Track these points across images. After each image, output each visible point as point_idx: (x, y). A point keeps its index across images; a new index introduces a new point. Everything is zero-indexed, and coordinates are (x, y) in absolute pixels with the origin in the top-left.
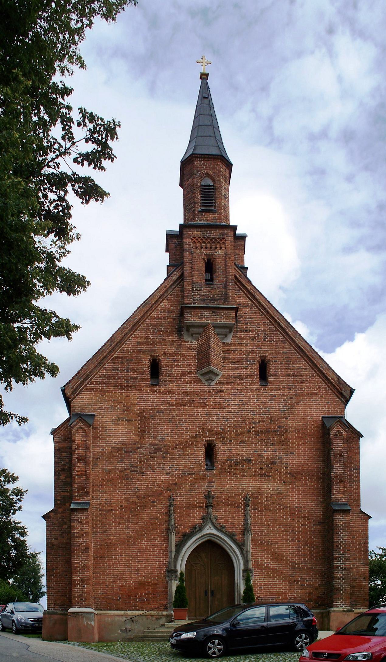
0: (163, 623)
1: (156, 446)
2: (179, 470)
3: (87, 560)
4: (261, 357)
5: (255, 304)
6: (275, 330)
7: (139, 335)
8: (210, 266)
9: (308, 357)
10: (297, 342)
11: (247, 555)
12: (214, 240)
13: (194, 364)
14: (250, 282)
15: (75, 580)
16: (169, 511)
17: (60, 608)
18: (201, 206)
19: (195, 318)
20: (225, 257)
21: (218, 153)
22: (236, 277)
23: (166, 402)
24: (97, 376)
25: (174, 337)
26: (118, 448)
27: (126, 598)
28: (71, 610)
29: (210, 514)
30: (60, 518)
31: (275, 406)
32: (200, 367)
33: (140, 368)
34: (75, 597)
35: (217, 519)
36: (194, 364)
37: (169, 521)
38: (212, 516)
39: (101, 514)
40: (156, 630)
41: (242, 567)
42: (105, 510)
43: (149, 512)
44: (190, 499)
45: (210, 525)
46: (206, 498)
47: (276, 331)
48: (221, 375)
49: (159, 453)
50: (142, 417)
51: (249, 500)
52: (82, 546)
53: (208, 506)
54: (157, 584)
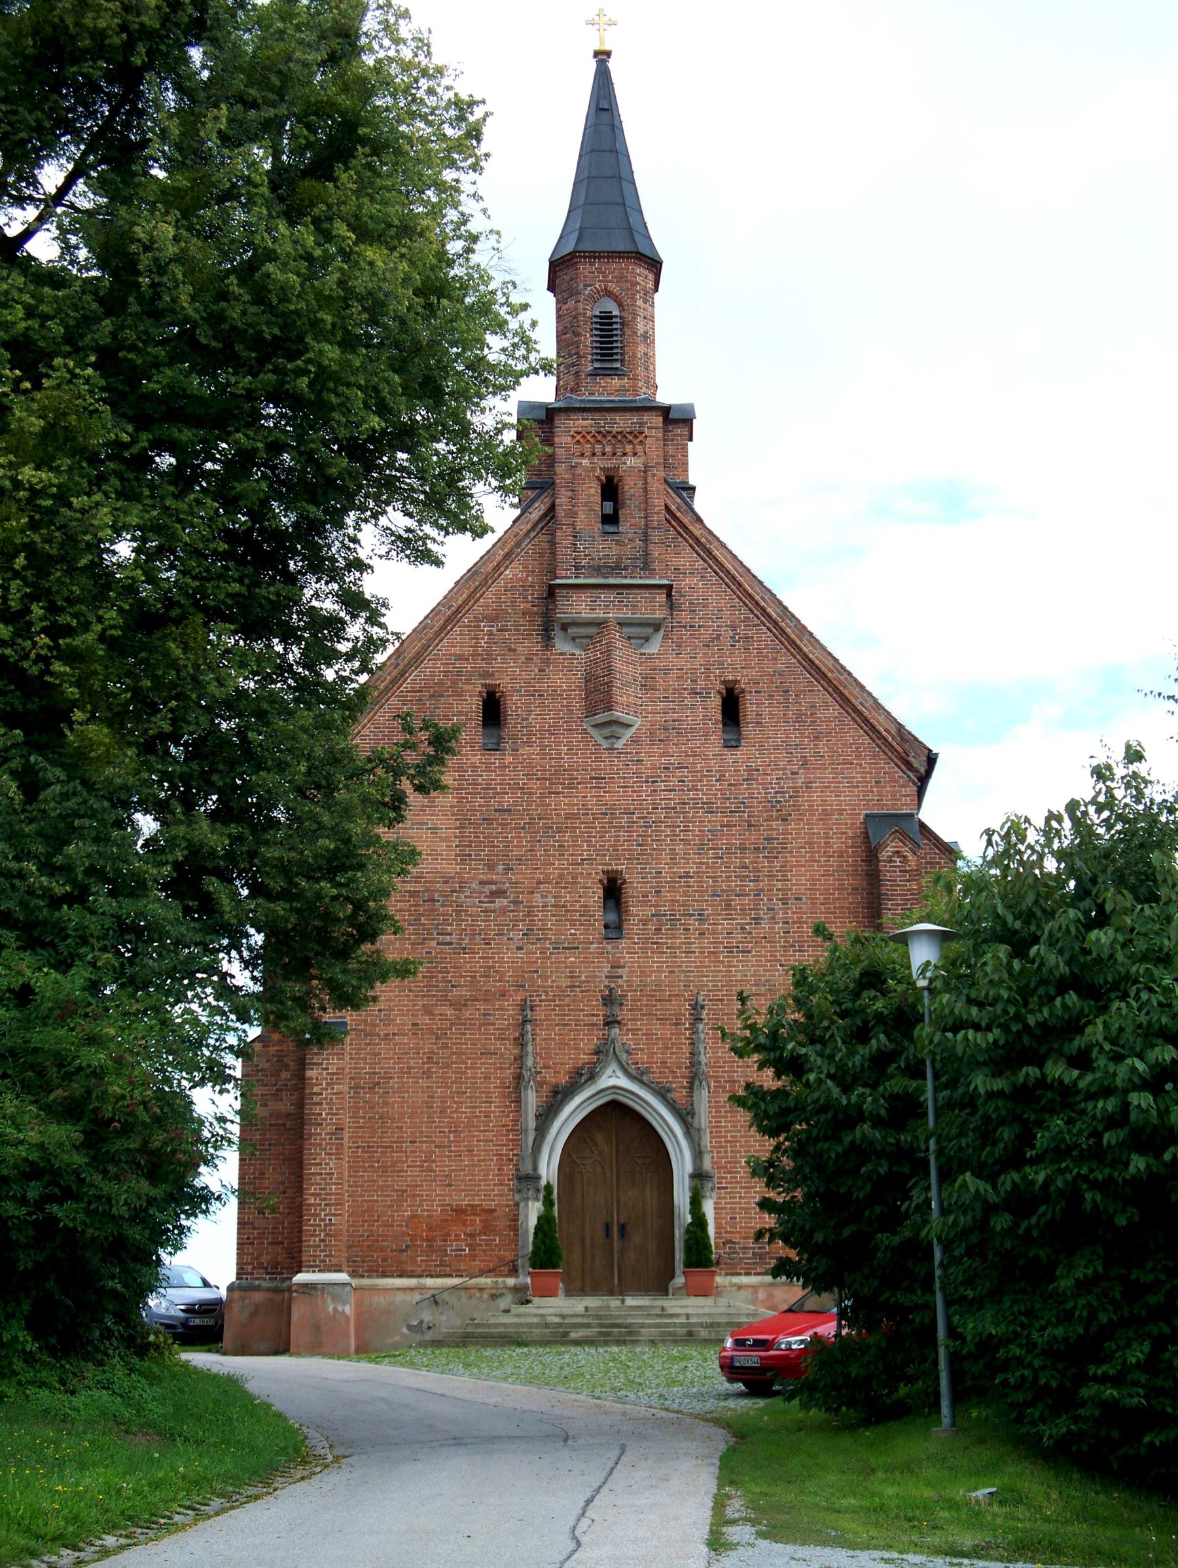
0: (507, 1308)
1: (494, 887)
2: (546, 939)
3: (339, 1156)
4: (725, 682)
5: (711, 567)
6: (756, 622)
7: (457, 640)
8: (610, 489)
9: (829, 682)
10: (805, 649)
11: (700, 1138)
12: (621, 437)
13: (577, 703)
14: (699, 520)
15: (310, 1205)
16: (523, 1035)
17: (268, 1274)
18: (592, 361)
19: (579, 607)
20: (645, 472)
21: (631, 248)
22: (667, 508)
23: (516, 788)
24: (365, 731)
25: (533, 644)
26: (409, 891)
27: (421, 1246)
28: (300, 1278)
29: (613, 1041)
30: (273, 1056)
31: (758, 791)
32: (591, 711)
33: (460, 713)
34: (308, 1246)
35: (630, 1054)
36: (577, 704)
37: (520, 1059)
38: (618, 1046)
39: (368, 1044)
40: (492, 1321)
41: (689, 1168)
42: (379, 1035)
43: (478, 1039)
44: (569, 1005)
45: (614, 1066)
46: (604, 1005)
47: (757, 625)
48: (637, 726)
49: (500, 902)
50: (463, 823)
51: (702, 1007)
52: (327, 1124)
53: (609, 1023)
54: (495, 1210)
